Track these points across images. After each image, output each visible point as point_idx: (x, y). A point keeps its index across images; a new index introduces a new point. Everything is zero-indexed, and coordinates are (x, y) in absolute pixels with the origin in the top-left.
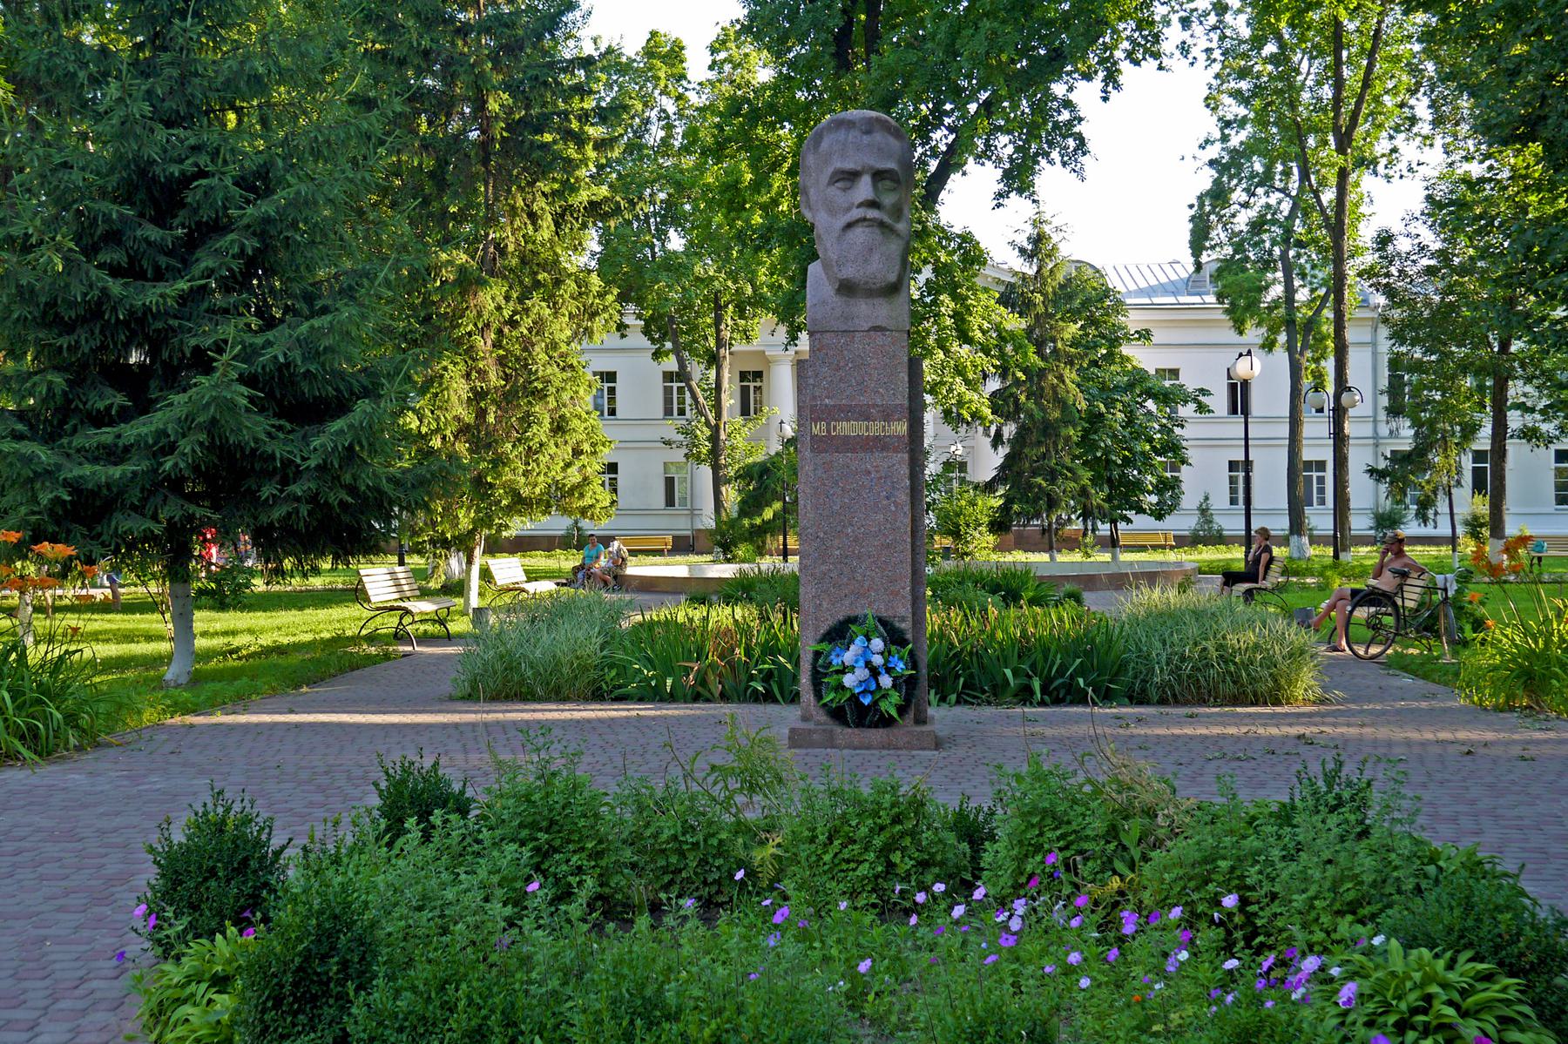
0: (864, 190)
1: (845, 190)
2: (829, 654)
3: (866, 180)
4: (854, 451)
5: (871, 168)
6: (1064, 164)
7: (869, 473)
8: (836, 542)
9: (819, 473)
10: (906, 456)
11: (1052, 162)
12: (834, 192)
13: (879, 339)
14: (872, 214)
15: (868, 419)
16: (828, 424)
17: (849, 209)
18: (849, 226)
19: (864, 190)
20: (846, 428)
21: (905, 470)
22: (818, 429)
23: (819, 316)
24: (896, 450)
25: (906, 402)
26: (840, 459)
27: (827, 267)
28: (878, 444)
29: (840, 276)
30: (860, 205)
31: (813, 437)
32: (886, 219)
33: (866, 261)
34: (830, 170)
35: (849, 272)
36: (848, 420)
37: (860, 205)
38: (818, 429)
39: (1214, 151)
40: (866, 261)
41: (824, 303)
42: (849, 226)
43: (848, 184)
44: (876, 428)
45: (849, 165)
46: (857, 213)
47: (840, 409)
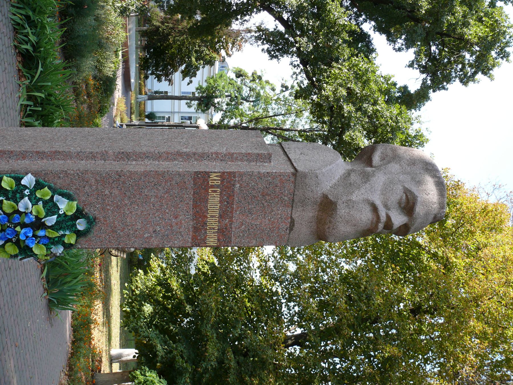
1: (399, 203)
4: (195, 206)
7: (176, 218)
8: (116, 192)
13: (284, 226)
14: (381, 226)
15: (221, 216)
16: (218, 186)
17: (386, 206)
18: (375, 209)
23: (307, 181)
26: (189, 196)
29: (340, 202)
35: (342, 211)
36: (221, 202)
37: (388, 218)
40: (347, 222)
43: (403, 205)
47: (231, 196)
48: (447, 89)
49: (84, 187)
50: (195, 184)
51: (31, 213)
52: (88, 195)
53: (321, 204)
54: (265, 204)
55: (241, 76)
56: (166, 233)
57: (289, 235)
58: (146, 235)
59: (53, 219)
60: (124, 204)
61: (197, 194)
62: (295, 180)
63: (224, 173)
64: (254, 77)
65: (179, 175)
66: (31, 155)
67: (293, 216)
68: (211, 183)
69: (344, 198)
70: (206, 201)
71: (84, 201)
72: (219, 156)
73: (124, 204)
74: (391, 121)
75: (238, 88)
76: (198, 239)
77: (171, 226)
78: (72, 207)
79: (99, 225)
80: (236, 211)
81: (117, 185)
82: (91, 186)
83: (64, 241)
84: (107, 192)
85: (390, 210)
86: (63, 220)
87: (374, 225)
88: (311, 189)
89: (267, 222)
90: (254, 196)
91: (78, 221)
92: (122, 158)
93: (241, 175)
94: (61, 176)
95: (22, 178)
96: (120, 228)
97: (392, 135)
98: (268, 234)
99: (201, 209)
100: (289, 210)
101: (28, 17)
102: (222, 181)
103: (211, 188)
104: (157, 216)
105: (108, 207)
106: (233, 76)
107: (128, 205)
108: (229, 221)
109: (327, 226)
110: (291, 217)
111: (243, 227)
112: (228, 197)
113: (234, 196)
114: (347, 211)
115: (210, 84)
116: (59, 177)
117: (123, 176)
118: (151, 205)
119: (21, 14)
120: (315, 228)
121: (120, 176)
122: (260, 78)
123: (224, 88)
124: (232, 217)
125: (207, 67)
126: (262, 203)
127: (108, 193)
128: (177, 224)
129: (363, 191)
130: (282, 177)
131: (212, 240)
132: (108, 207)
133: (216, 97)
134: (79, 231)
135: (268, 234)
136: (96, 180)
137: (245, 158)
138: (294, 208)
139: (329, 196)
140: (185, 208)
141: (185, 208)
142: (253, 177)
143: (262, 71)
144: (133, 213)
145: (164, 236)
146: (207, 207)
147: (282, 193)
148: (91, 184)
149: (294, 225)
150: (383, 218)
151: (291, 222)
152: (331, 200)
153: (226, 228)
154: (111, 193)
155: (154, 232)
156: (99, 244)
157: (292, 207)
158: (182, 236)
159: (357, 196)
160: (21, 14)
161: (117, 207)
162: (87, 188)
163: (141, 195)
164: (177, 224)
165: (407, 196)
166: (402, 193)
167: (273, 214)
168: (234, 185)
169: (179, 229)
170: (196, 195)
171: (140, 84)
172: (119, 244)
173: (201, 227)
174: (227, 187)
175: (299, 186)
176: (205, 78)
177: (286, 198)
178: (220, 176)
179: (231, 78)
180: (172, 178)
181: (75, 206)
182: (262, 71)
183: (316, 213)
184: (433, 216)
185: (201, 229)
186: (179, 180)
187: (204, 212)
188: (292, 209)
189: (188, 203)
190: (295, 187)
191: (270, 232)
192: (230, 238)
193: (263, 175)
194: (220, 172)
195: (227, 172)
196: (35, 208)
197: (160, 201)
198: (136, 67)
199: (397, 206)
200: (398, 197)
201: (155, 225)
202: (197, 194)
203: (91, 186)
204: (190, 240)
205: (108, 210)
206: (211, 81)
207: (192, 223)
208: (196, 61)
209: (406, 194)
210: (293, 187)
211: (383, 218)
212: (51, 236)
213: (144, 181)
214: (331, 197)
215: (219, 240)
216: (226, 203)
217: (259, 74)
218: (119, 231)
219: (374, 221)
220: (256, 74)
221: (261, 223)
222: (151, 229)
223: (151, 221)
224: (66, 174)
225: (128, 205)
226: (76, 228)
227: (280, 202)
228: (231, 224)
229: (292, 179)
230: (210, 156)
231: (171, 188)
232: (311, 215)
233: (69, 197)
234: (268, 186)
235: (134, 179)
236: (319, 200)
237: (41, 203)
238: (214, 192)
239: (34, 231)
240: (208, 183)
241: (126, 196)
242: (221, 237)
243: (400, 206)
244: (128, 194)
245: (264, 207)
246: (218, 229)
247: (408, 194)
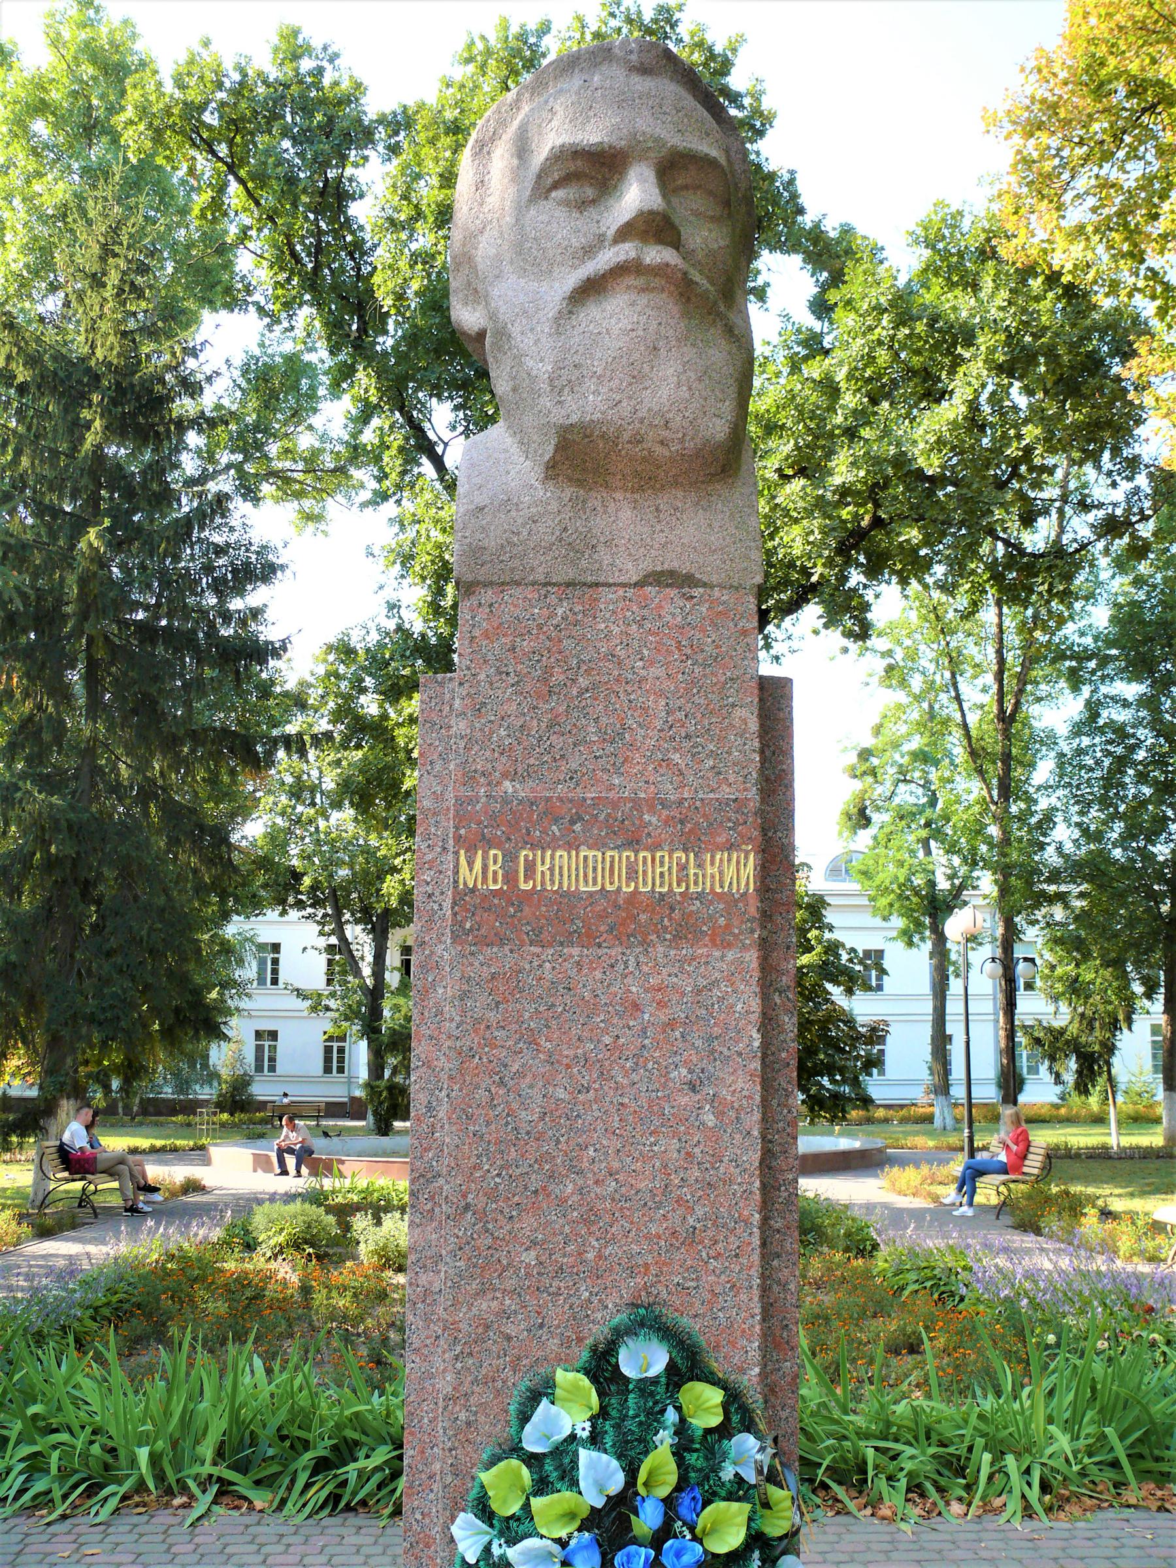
1: (582, 205)
4: (589, 938)
5: (657, 140)
8: (527, 1224)
9: (480, 1002)
10: (752, 958)
14: (655, 255)
15: (633, 842)
16: (510, 858)
17: (589, 251)
23: (491, 543)
25: (753, 793)
29: (558, 416)
31: (463, 897)
33: (637, 378)
36: (572, 845)
37: (625, 233)
40: (637, 378)
43: (590, 192)
45: (593, 135)
46: (608, 258)
48: (792, 172)
49: (509, 1338)
50: (501, 941)
51: (563, 1543)
52: (541, 1326)
53: (580, 483)
54: (583, 682)
55: (862, 811)
56: (699, 1043)
57: (712, 587)
58: (710, 1119)
59: (592, 1465)
60: (576, 1198)
61: (538, 931)
62: (491, 583)
63: (458, 839)
64: (864, 773)
65: (464, 996)
66: (418, 1516)
67: (635, 579)
68: (495, 881)
69: (546, 402)
70: (568, 898)
71: (566, 1343)
72: (429, 857)
73: (576, 1198)
74: (879, 330)
75: (902, 818)
76: (728, 926)
77: (671, 1024)
78: (575, 1388)
79: (664, 1294)
80: (611, 787)
81: (502, 1221)
82: (505, 1314)
83: (708, 1431)
84: (530, 1257)
85: (603, 235)
86: (617, 1427)
87: (657, 282)
88: (524, 525)
89: (655, 671)
90: (550, 727)
91: (626, 1371)
92: (432, 1198)
93: (469, 778)
94: (463, 1416)
95: (463, 1559)
96: (675, 1218)
97: (920, 318)
98: (705, 666)
99: (603, 916)
100: (607, 595)
101: (321, 1466)
102: (490, 843)
103: (517, 881)
104: (626, 1075)
105: (590, 1256)
106: (865, 837)
107: (580, 1182)
108: (652, 809)
109: (659, 450)
110: (639, 584)
111: (676, 757)
112: (556, 821)
113: (549, 799)
114: (591, 384)
115: (891, 905)
116: (468, 1424)
117: (465, 1196)
118: (581, 1097)
119: (308, 1486)
120: (680, 494)
121: (467, 1207)
122: (865, 754)
123: (901, 864)
124: (636, 803)
125: (830, 917)
126: (580, 694)
127: (533, 1253)
128: (661, 1005)
130: (477, 633)
131: (729, 873)
132: (590, 1256)
133: (932, 884)
134: (671, 1367)
135: (705, 666)
136: (481, 1293)
137: (438, 767)
138: (602, 579)
139: (547, 457)
140: (598, 975)
141: (598, 975)
142: (478, 735)
143: (845, 750)
144: (616, 1165)
145: (713, 1051)
146: (591, 894)
147: (540, 626)
148: (497, 1314)
149: (672, 573)
150: (626, 251)
151: (659, 583)
152: (557, 449)
153: (682, 822)
154: (534, 1243)
155: (693, 1089)
156: (743, 1297)
157: (597, 585)
158: (715, 983)
159: (542, 360)
160: (308, 1486)
161: (586, 1222)
162: (511, 1330)
163: (542, 1134)
164: (661, 1005)
165: (555, 186)
166: (548, 205)
167: (622, 654)
168: (506, 801)
169: (683, 994)
170: (545, 936)
171: (904, 1121)
172: (746, 1222)
173: (677, 915)
174: (514, 826)
175: (512, 570)
176: (878, 922)
177: (560, 611)
178: (471, 850)
179: (871, 843)
180: (478, 1021)
181: (571, 1375)
182: (845, 750)
183: (618, 495)
184: (636, 79)
185: (686, 916)
186: (484, 999)
187: (616, 906)
188: (610, 585)
189: (578, 963)
190: (518, 584)
191: (700, 658)
192: (723, 803)
193: (468, 701)
194: (457, 853)
195: (457, 828)
196: (546, 1525)
197: (568, 1066)
198: (841, 1134)
199: (592, 212)
200: (560, 213)
201: (664, 1086)
202: (538, 931)
203: (505, 1314)
204: (730, 955)
205: (600, 1256)
206: (883, 902)
207: (661, 949)
208: (810, 949)
209: (550, 190)
210: (517, 591)
211: (626, 251)
212: (673, 1479)
213: (488, 1124)
214: (549, 451)
215: (730, 847)
216: (578, 827)
217: (853, 758)
218: (691, 1221)
219: (640, 282)
220: (853, 768)
221: (661, 694)
222: (683, 1100)
223: (650, 1100)
224: (455, 1399)
225: (580, 1182)
226: (655, 1381)
227: (577, 631)
228: (664, 804)
229: (488, 595)
230: (429, 889)
231: (514, 1027)
232: (626, 514)
233: (542, 1391)
234: (512, 679)
235: (478, 1156)
236: (569, 492)
237: (536, 1502)
238: (534, 872)
239: (635, 1541)
240: (495, 893)
241: (544, 1188)
242: (721, 839)
243: (593, 201)
244: (535, 1182)
245: (594, 686)
246: (685, 850)
247: (550, 181)
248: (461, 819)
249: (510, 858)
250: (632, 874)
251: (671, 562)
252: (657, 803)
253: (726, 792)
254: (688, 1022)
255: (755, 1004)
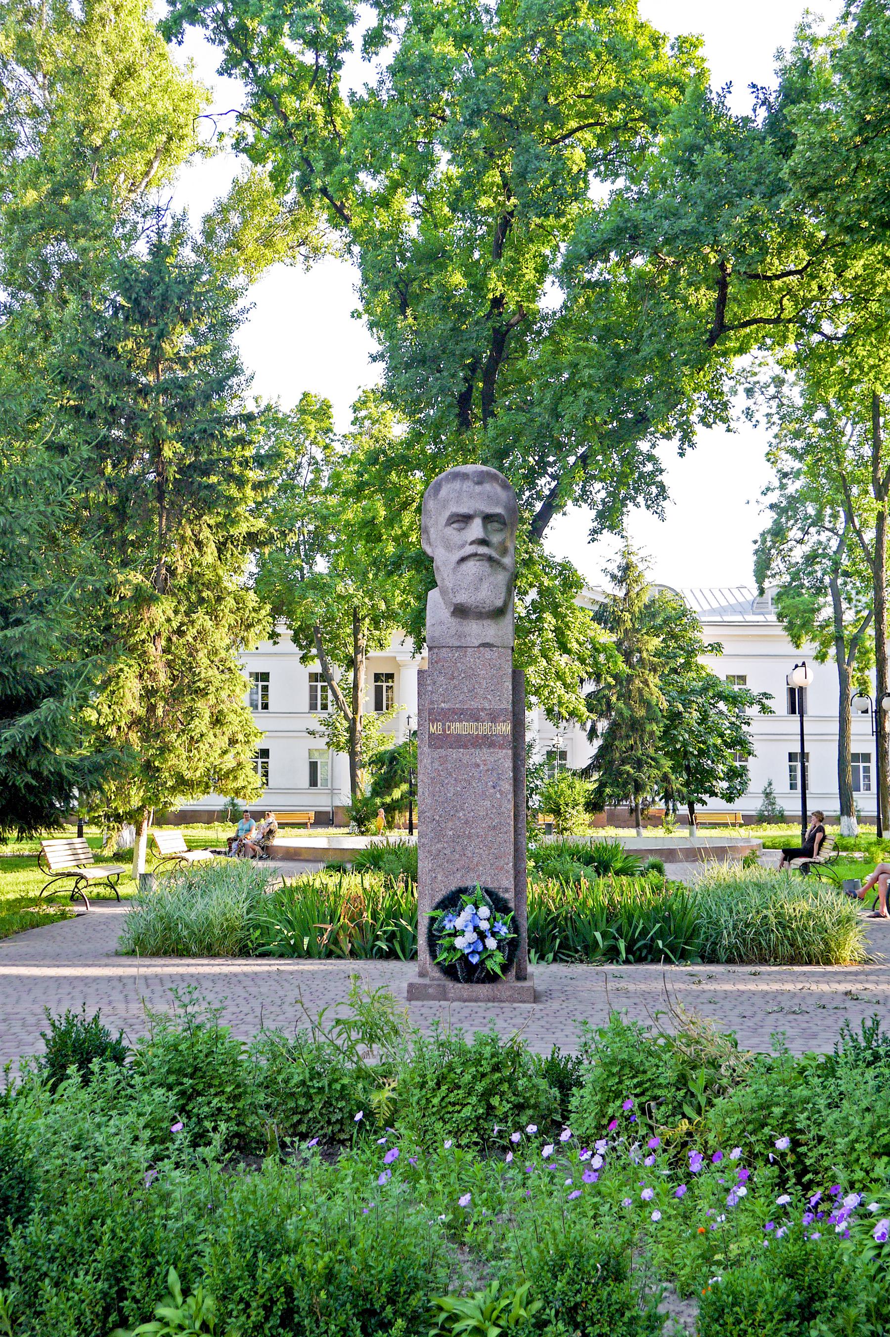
0: (476, 529)
1: (460, 530)
2: (443, 920)
3: (477, 522)
4: (465, 747)
5: (482, 512)
6: (648, 507)
8: (450, 824)
9: (436, 765)
10: (510, 752)
11: (637, 505)
12: (451, 532)
13: (487, 653)
15: (477, 720)
16: (444, 724)
17: (463, 546)
18: (463, 560)
19: (476, 529)
20: (459, 728)
21: (509, 764)
22: (435, 728)
23: (437, 634)
24: (501, 747)
25: (510, 707)
26: (454, 754)
27: (443, 593)
28: (488, 742)
29: (455, 601)
30: (472, 543)
31: (431, 735)
32: (494, 554)
33: (476, 589)
34: (447, 514)
35: (462, 598)
36: (461, 721)
37: (472, 543)
38: (435, 728)
39: (774, 497)
40: (476, 589)
41: (441, 623)
42: (463, 560)
43: (462, 525)
44: (484, 728)
45: (463, 510)
46: (469, 550)
47: (454, 711)
77: (488, 770)
82: (444, 848)
84: (451, 833)
129: (445, 576)
174: (445, 715)
203: (444, 848)
229: (436, 650)
232: (474, 626)
248: (430, 714)
249: (444, 724)
250: (477, 729)
251: (487, 641)
252: (483, 709)
253: (503, 706)
254: (493, 770)
255: (511, 765)
